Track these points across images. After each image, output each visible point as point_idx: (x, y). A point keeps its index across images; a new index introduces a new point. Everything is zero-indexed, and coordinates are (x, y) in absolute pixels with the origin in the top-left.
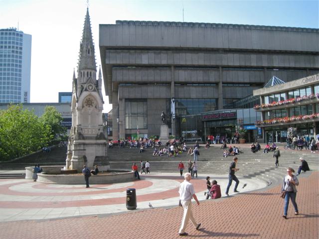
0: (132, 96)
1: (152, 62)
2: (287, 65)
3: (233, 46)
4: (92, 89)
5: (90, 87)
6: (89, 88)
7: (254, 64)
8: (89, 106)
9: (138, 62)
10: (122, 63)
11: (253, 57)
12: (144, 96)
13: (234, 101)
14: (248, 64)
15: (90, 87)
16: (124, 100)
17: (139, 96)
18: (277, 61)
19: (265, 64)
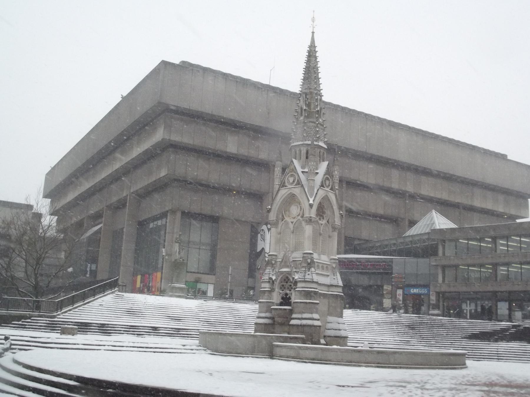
0: (195, 208)
1: (244, 151)
2: (439, 196)
3: (373, 150)
4: (329, 185)
5: (327, 182)
6: (325, 184)
7: (395, 186)
8: (320, 219)
9: (220, 146)
10: (191, 142)
11: (395, 173)
12: (217, 212)
13: (356, 242)
14: (387, 184)
15: (327, 182)
16: (179, 215)
17: (207, 210)
18: (427, 188)
19: (410, 188)
